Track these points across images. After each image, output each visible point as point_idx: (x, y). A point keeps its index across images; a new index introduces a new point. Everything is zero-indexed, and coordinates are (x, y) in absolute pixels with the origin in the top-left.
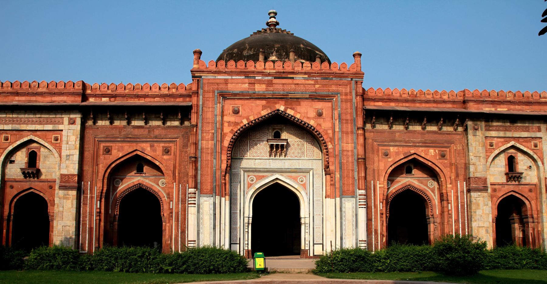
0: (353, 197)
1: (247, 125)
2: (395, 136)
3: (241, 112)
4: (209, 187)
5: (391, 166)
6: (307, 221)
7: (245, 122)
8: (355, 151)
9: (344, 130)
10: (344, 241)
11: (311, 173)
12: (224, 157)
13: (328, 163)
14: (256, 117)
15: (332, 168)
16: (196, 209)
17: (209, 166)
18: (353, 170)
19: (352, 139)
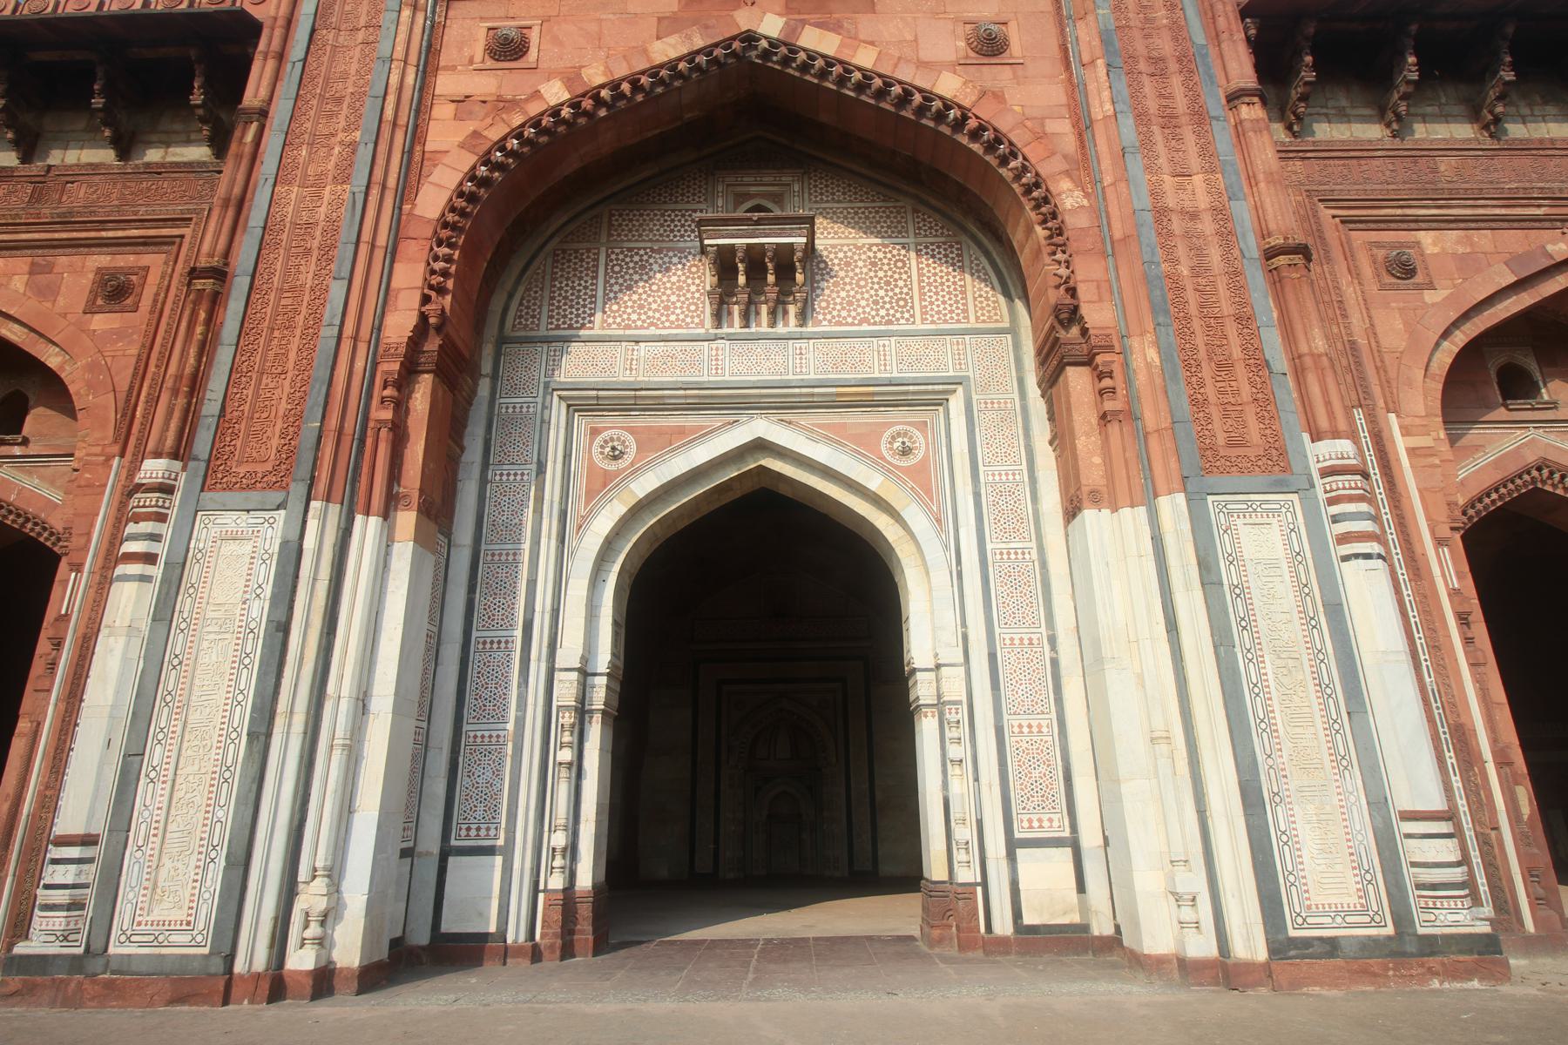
0: (1280, 487)
1: (566, 112)
2: (1435, 171)
3: (532, 55)
4: (275, 442)
5: (1446, 335)
6: (954, 688)
7: (556, 93)
8: (1242, 211)
9: (1152, 105)
10: (1278, 818)
11: (956, 403)
12: (410, 276)
13: (1072, 292)
14: (621, 71)
15: (1097, 315)
16: (151, 592)
17: (300, 319)
18: (1245, 320)
19: (1206, 151)
